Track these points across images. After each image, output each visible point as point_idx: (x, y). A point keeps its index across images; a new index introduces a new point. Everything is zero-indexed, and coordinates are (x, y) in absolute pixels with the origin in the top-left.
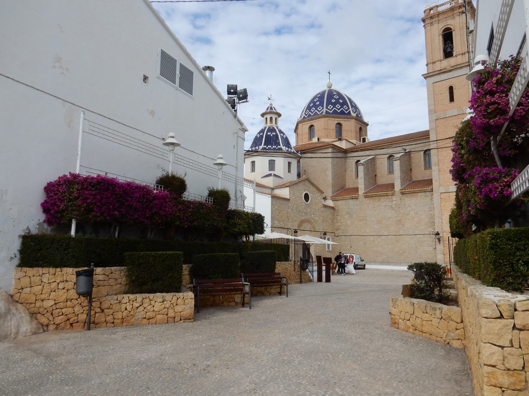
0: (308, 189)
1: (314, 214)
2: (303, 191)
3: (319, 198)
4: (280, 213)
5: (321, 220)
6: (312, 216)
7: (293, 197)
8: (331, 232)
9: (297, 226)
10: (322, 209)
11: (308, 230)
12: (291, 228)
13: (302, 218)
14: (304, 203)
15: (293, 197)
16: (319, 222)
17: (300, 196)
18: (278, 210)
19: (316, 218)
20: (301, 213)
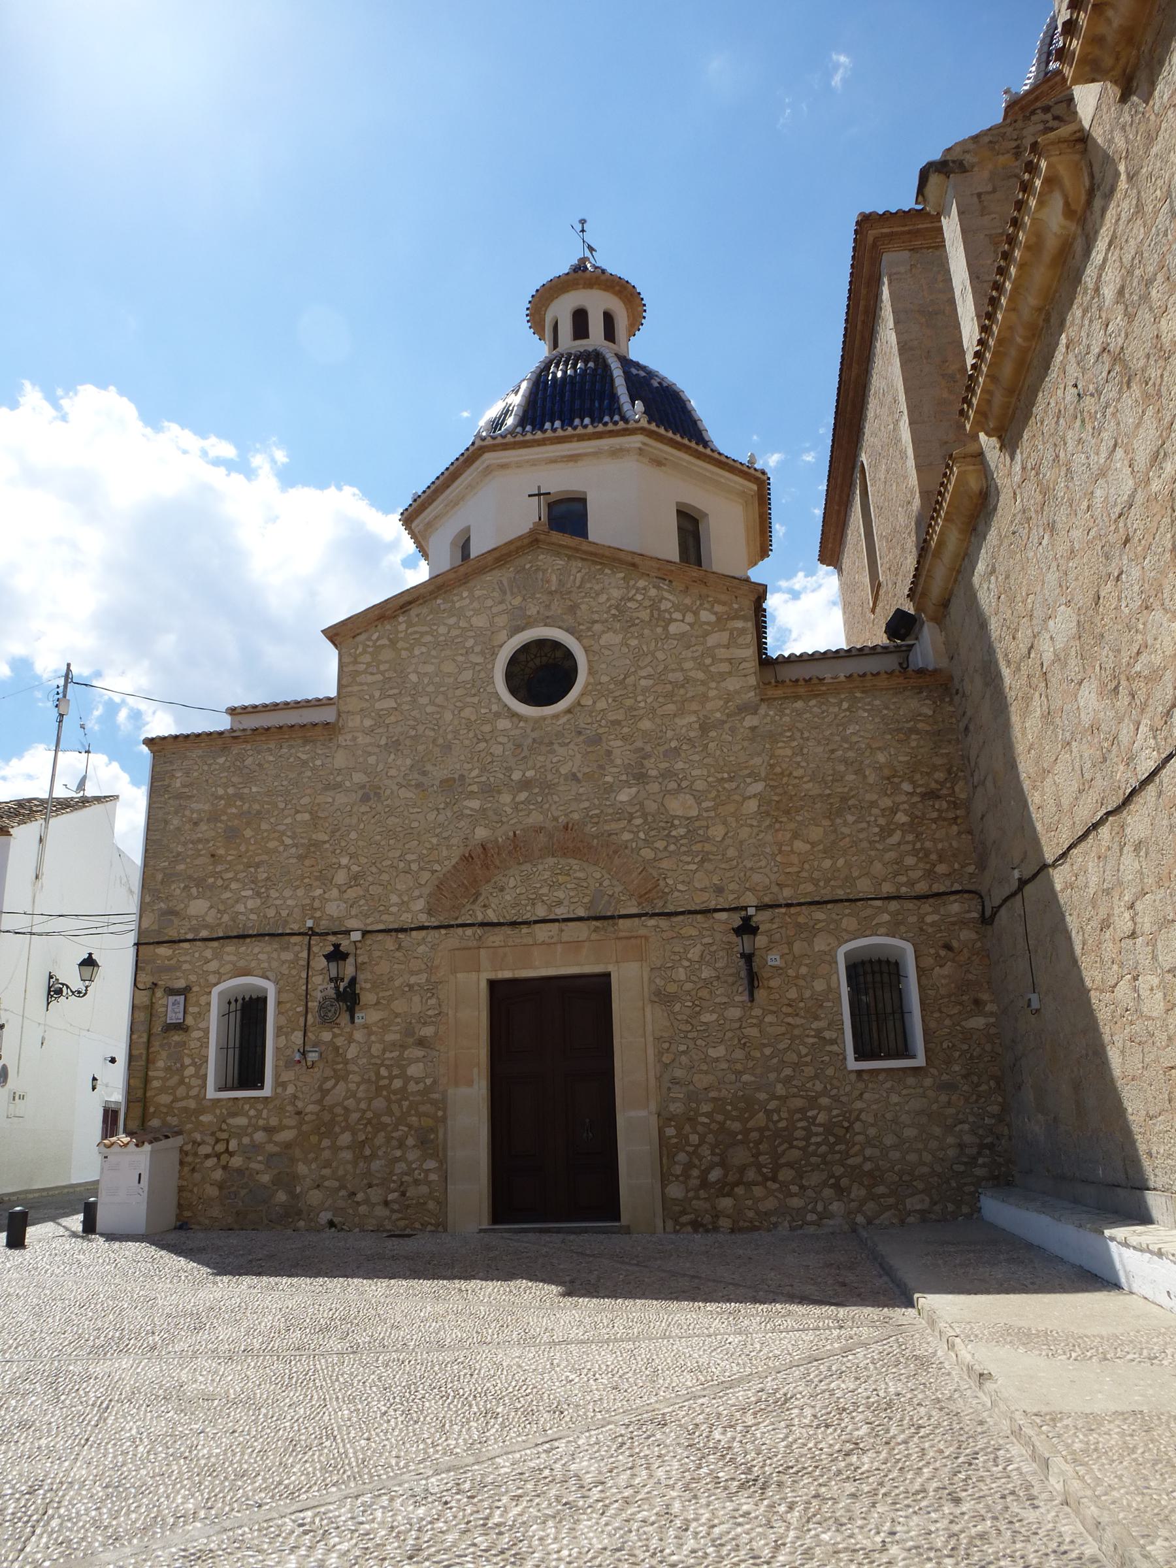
0: (557, 608)
1: (641, 778)
2: (503, 635)
3: (711, 641)
4: (232, 835)
5: (752, 806)
6: (624, 796)
7: (391, 703)
8: (922, 887)
9: (420, 904)
10: (750, 721)
11: (561, 912)
12: (351, 924)
13: (481, 833)
14: (514, 715)
15: (391, 703)
16: (717, 832)
17: (467, 675)
18: (214, 818)
19: (680, 806)
20: (471, 795)
